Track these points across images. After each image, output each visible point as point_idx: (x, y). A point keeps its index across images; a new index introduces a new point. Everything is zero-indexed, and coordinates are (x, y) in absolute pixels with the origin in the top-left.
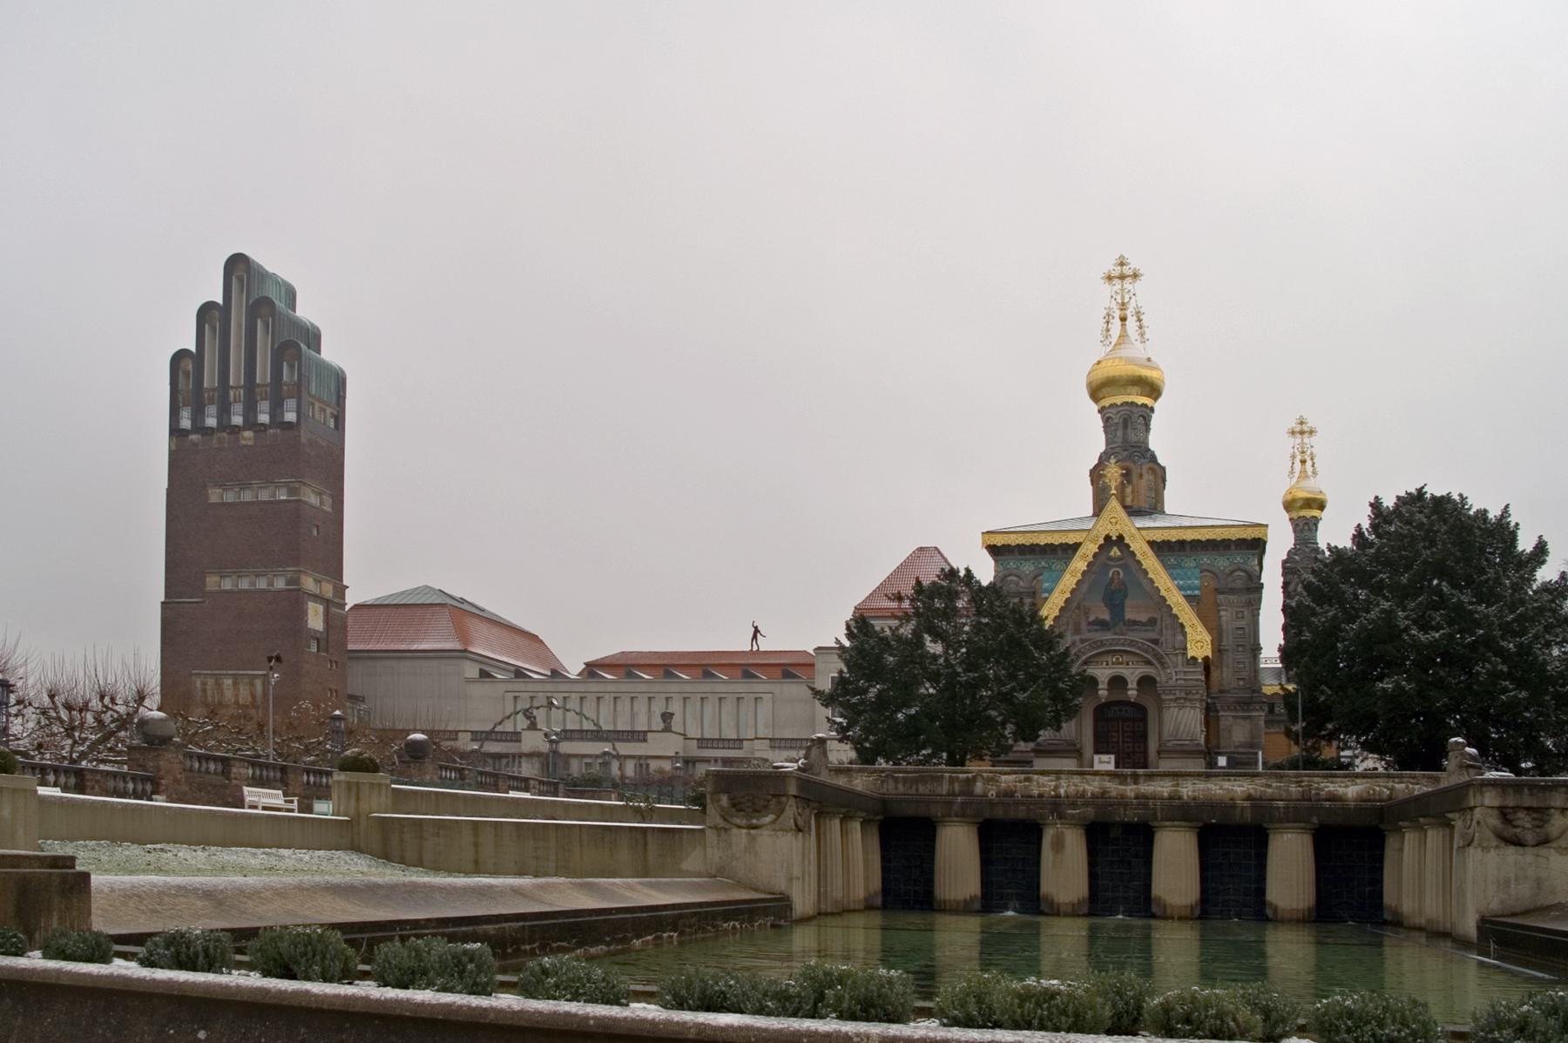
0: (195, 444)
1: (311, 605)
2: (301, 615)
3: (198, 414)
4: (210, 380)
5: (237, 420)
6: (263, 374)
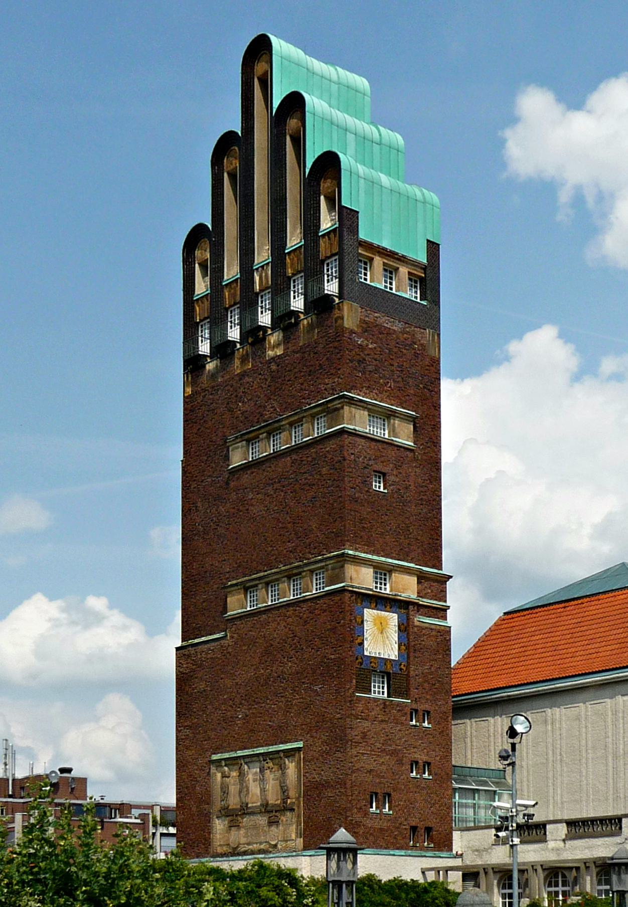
1: (370, 614)
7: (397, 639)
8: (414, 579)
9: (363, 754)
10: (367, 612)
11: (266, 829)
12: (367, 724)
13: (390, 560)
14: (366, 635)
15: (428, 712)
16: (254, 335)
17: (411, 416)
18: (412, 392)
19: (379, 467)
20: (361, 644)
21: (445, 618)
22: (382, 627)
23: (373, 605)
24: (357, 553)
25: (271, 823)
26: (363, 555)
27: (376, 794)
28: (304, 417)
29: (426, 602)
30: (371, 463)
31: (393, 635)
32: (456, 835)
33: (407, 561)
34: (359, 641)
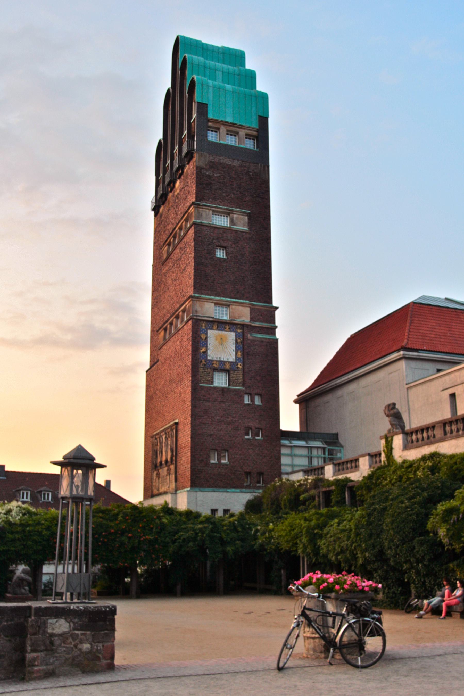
7: (234, 348)
9: (204, 423)
12: (207, 404)
13: (229, 299)
14: (209, 346)
18: (247, 199)
19: (222, 243)
20: (205, 352)
21: (274, 334)
22: (222, 341)
24: (203, 296)
26: (207, 297)
28: (182, 223)
29: (257, 324)
30: (214, 241)
31: (232, 347)
33: (243, 299)
34: (203, 350)
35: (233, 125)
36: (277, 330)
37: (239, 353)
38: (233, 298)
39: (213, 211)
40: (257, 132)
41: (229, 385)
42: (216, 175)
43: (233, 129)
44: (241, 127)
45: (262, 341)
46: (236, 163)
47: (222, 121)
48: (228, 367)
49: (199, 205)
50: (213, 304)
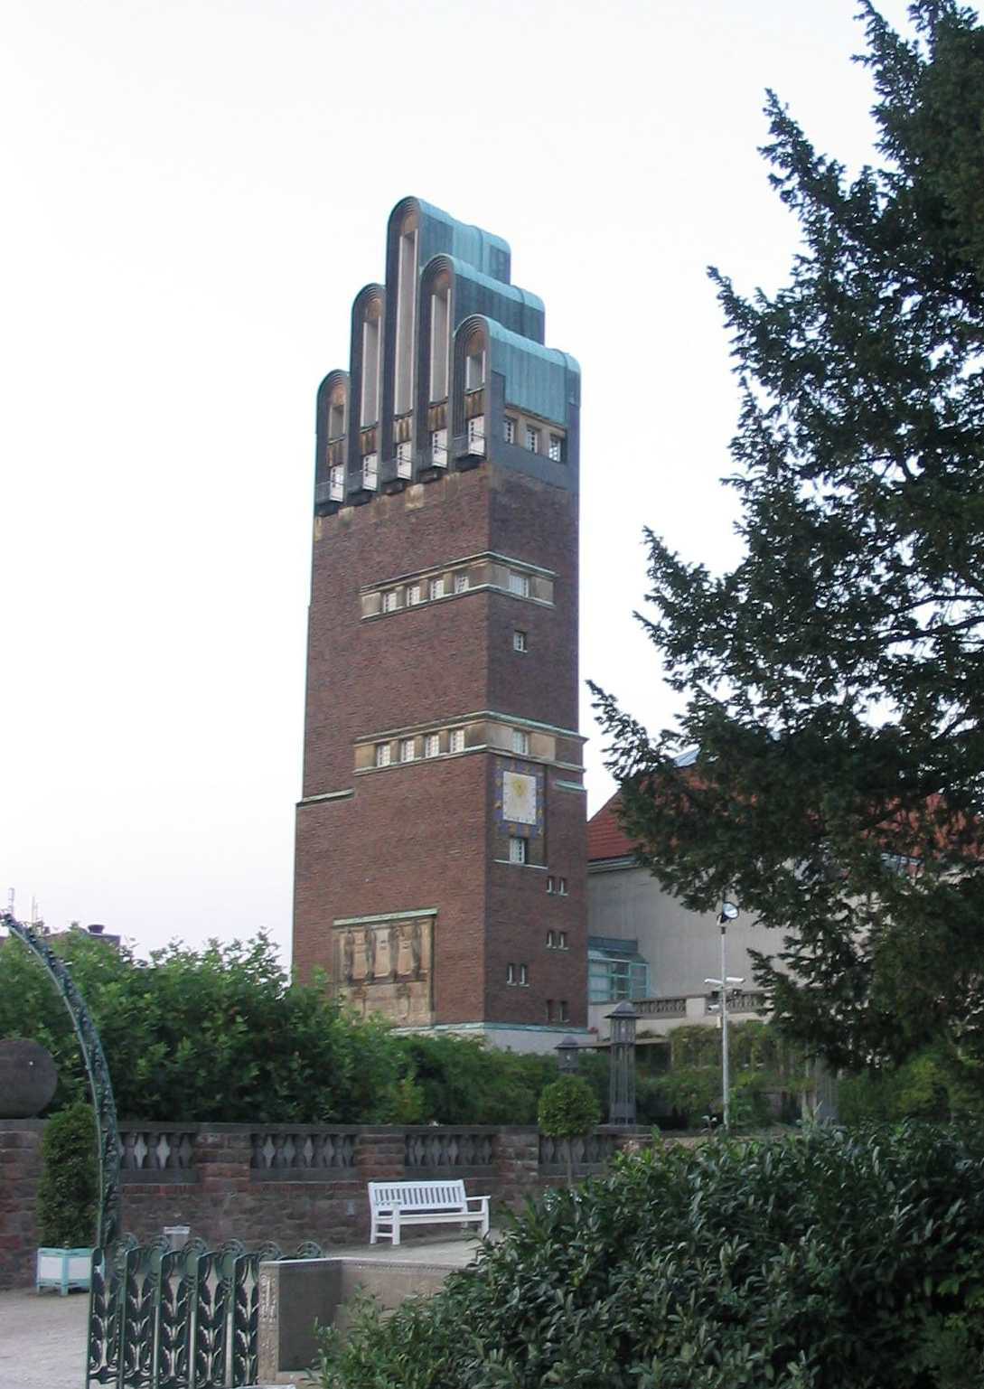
0: (346, 525)
1: (509, 777)
2: (493, 792)
3: (355, 466)
4: (370, 413)
5: (405, 471)
6: (440, 386)
8: (553, 739)
10: (505, 773)
11: (394, 1001)
13: (529, 722)
14: (506, 798)
15: (564, 880)
16: (393, 485)
17: (552, 576)
19: (521, 626)
20: (500, 808)
21: (580, 781)
23: (512, 768)
24: (498, 714)
25: (400, 995)
26: (503, 716)
27: (512, 965)
29: (563, 765)
31: (532, 800)
32: (591, 1009)
34: (498, 804)
35: (535, 416)
36: (585, 775)
37: (541, 811)
38: (538, 721)
39: (512, 570)
40: (566, 431)
41: (526, 862)
42: (513, 506)
43: (536, 421)
44: (546, 421)
45: (568, 794)
46: (538, 487)
47: (523, 409)
48: (526, 833)
49: (495, 558)
50: (511, 729)
